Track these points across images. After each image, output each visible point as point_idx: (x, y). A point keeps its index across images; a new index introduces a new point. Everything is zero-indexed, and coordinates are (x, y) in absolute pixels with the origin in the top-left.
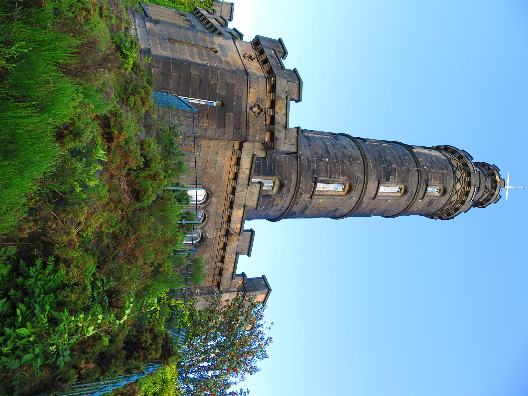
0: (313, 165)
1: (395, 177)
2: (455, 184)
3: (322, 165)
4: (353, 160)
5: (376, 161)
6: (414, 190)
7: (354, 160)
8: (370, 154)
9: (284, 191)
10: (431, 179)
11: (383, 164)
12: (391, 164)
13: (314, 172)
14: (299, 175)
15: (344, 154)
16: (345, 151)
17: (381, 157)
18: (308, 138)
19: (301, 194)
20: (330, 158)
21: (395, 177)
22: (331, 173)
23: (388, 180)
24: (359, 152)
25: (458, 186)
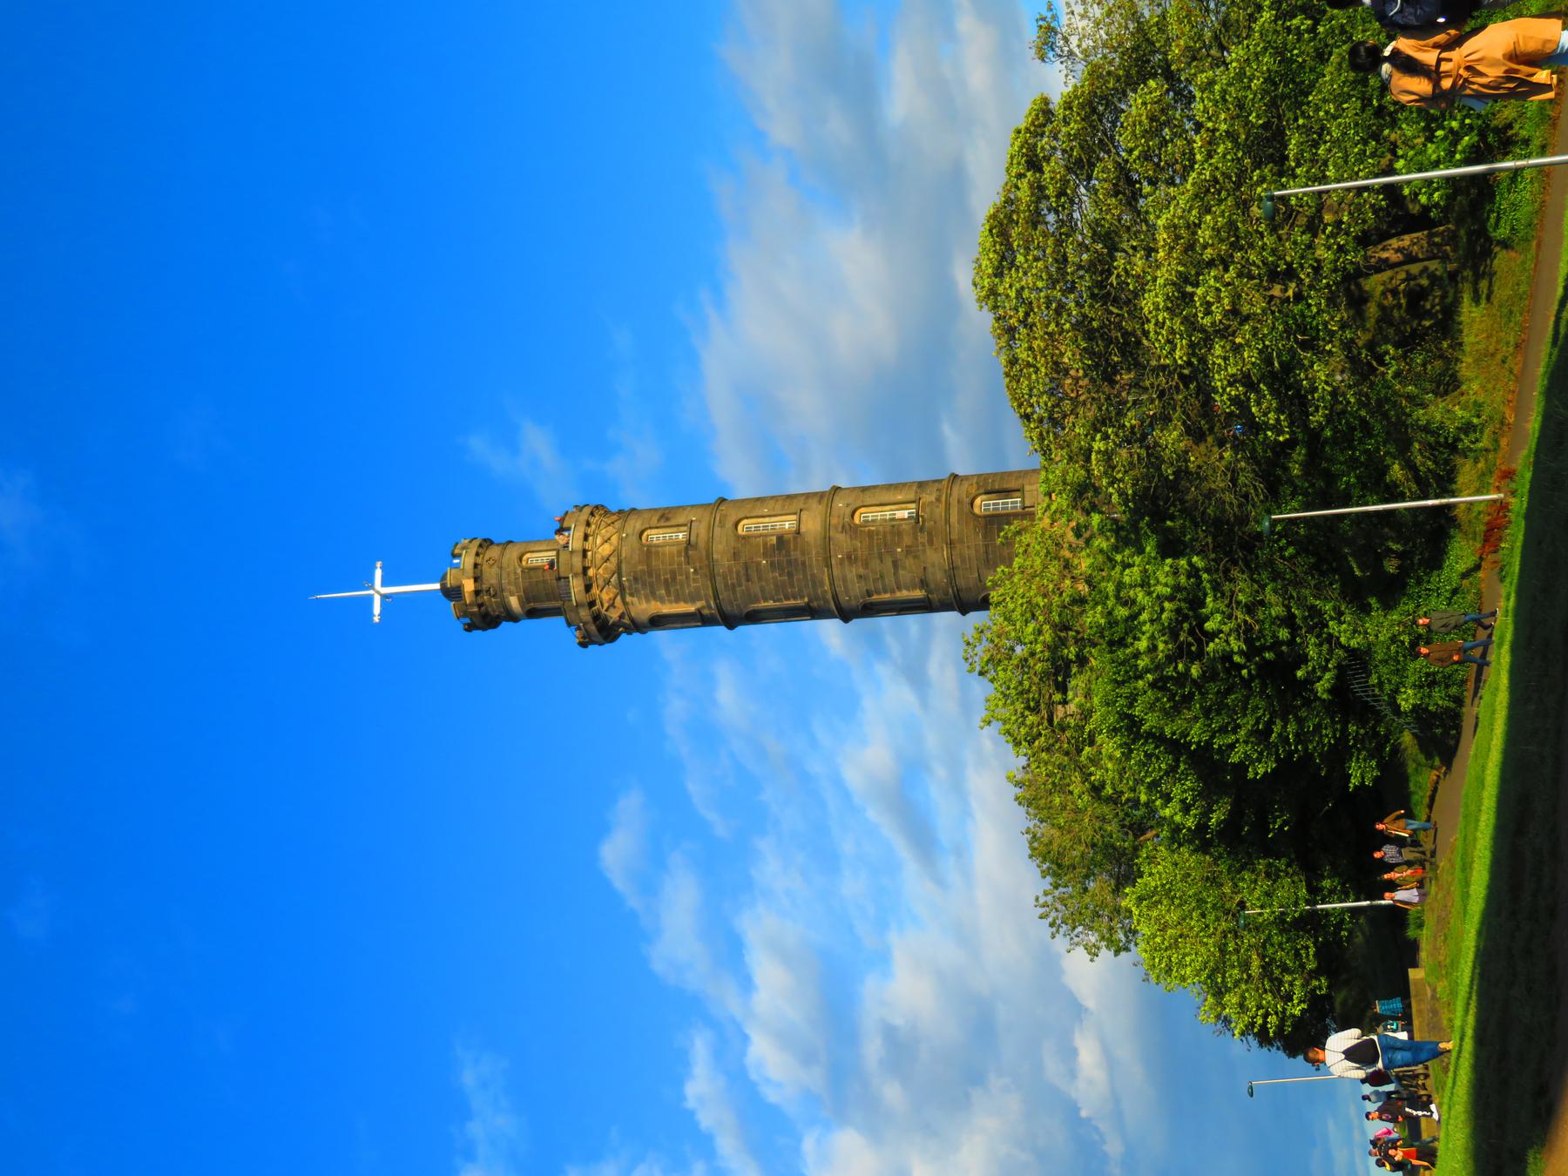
0: (922, 538)
1: (765, 544)
2: (617, 552)
3: (907, 540)
4: (850, 558)
5: (804, 563)
6: (717, 530)
7: (849, 557)
8: (813, 575)
9: (967, 500)
10: (679, 553)
11: (789, 562)
12: (772, 564)
13: (922, 530)
14: (947, 521)
15: (866, 565)
16: (861, 571)
17: (790, 575)
18: (923, 584)
19: (938, 500)
20: (892, 553)
21: (765, 544)
22: (892, 533)
23: (780, 538)
24: (836, 572)
25: (606, 550)
